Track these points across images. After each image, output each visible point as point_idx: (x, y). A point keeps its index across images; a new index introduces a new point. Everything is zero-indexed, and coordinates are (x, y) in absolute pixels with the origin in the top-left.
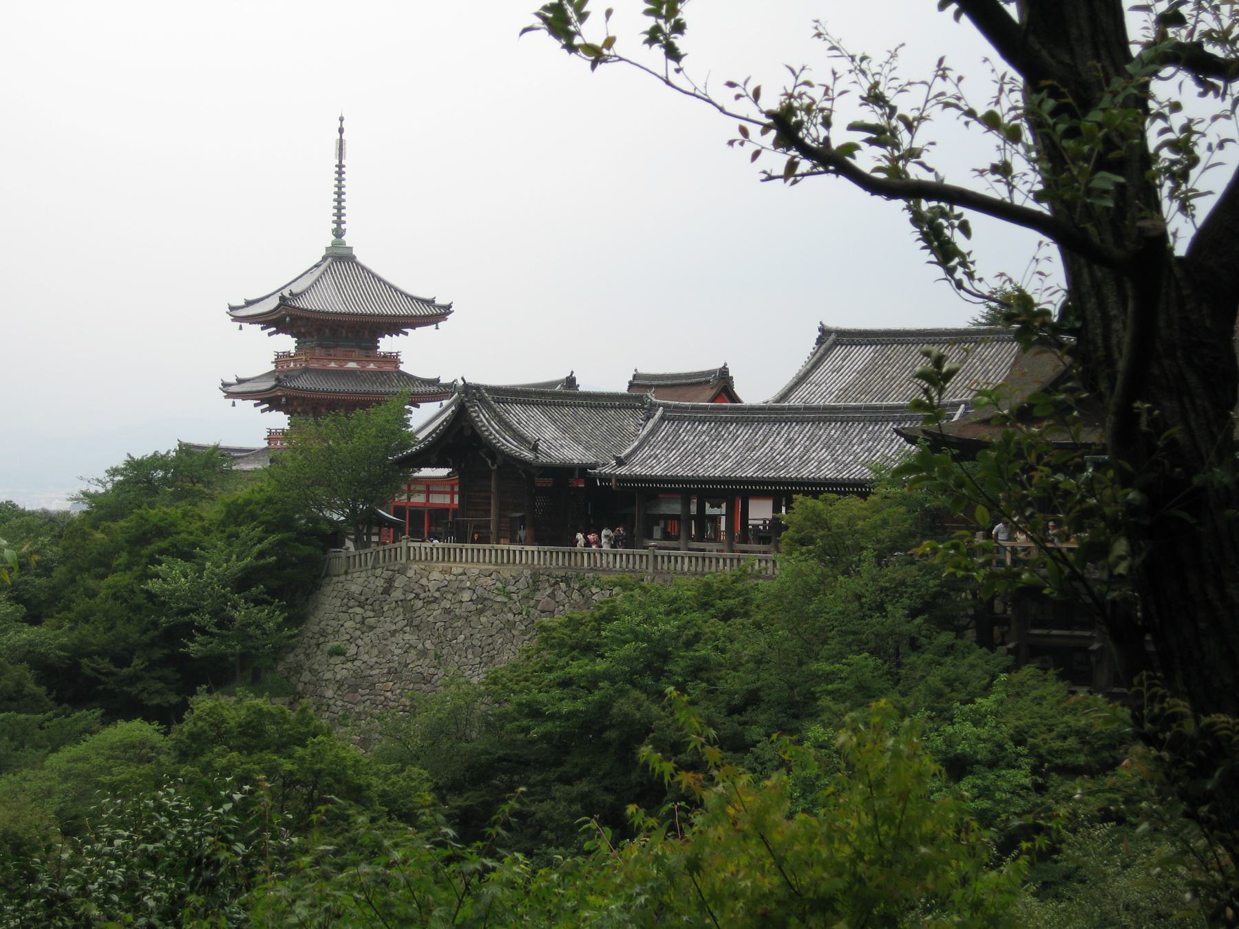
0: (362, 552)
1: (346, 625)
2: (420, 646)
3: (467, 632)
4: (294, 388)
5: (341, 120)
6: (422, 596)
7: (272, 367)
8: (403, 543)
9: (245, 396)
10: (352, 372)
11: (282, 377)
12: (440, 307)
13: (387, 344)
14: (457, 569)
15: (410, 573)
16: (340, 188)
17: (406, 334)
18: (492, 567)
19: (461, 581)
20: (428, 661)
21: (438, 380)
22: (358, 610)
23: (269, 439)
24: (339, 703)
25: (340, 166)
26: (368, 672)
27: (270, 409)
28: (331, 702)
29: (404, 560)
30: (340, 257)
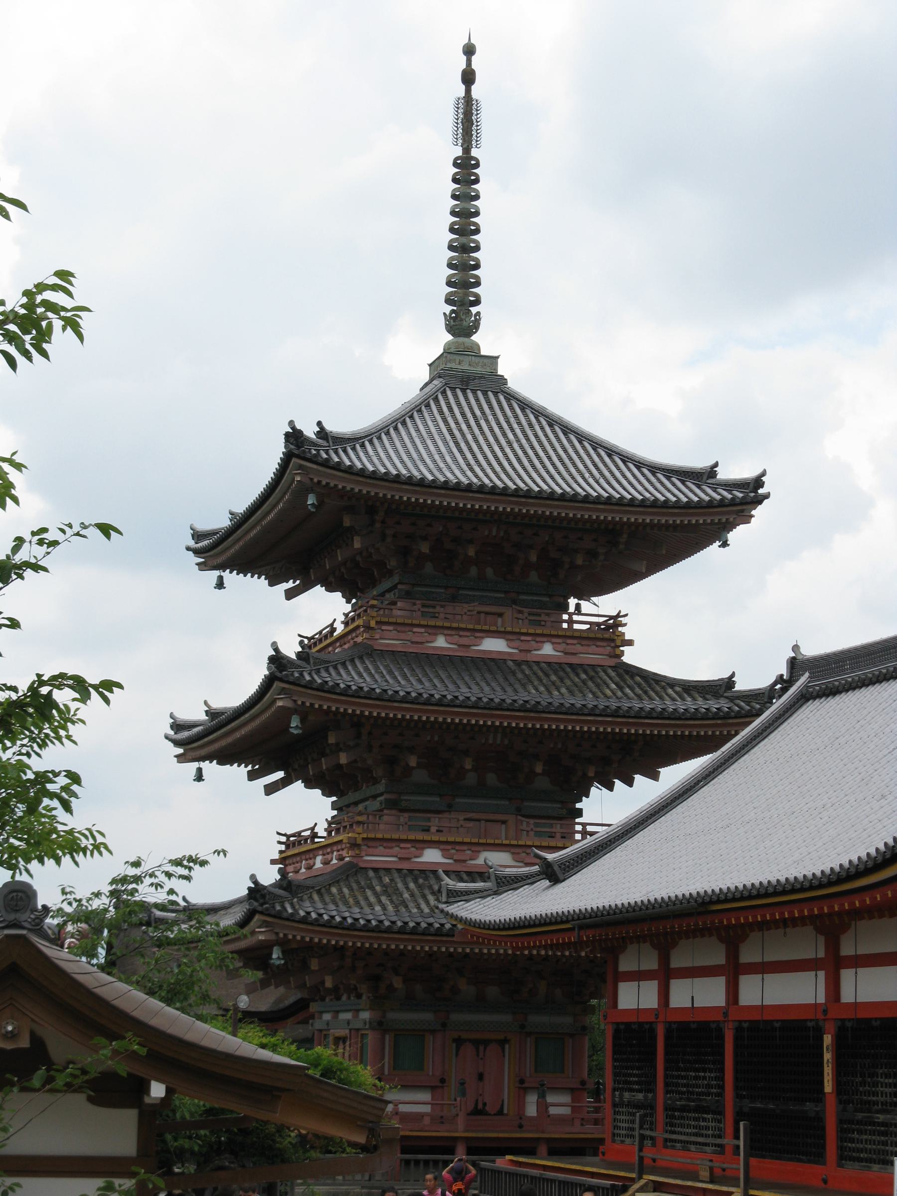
4: (321, 688)
10: (491, 665)
21: (729, 683)
30: (465, 376)
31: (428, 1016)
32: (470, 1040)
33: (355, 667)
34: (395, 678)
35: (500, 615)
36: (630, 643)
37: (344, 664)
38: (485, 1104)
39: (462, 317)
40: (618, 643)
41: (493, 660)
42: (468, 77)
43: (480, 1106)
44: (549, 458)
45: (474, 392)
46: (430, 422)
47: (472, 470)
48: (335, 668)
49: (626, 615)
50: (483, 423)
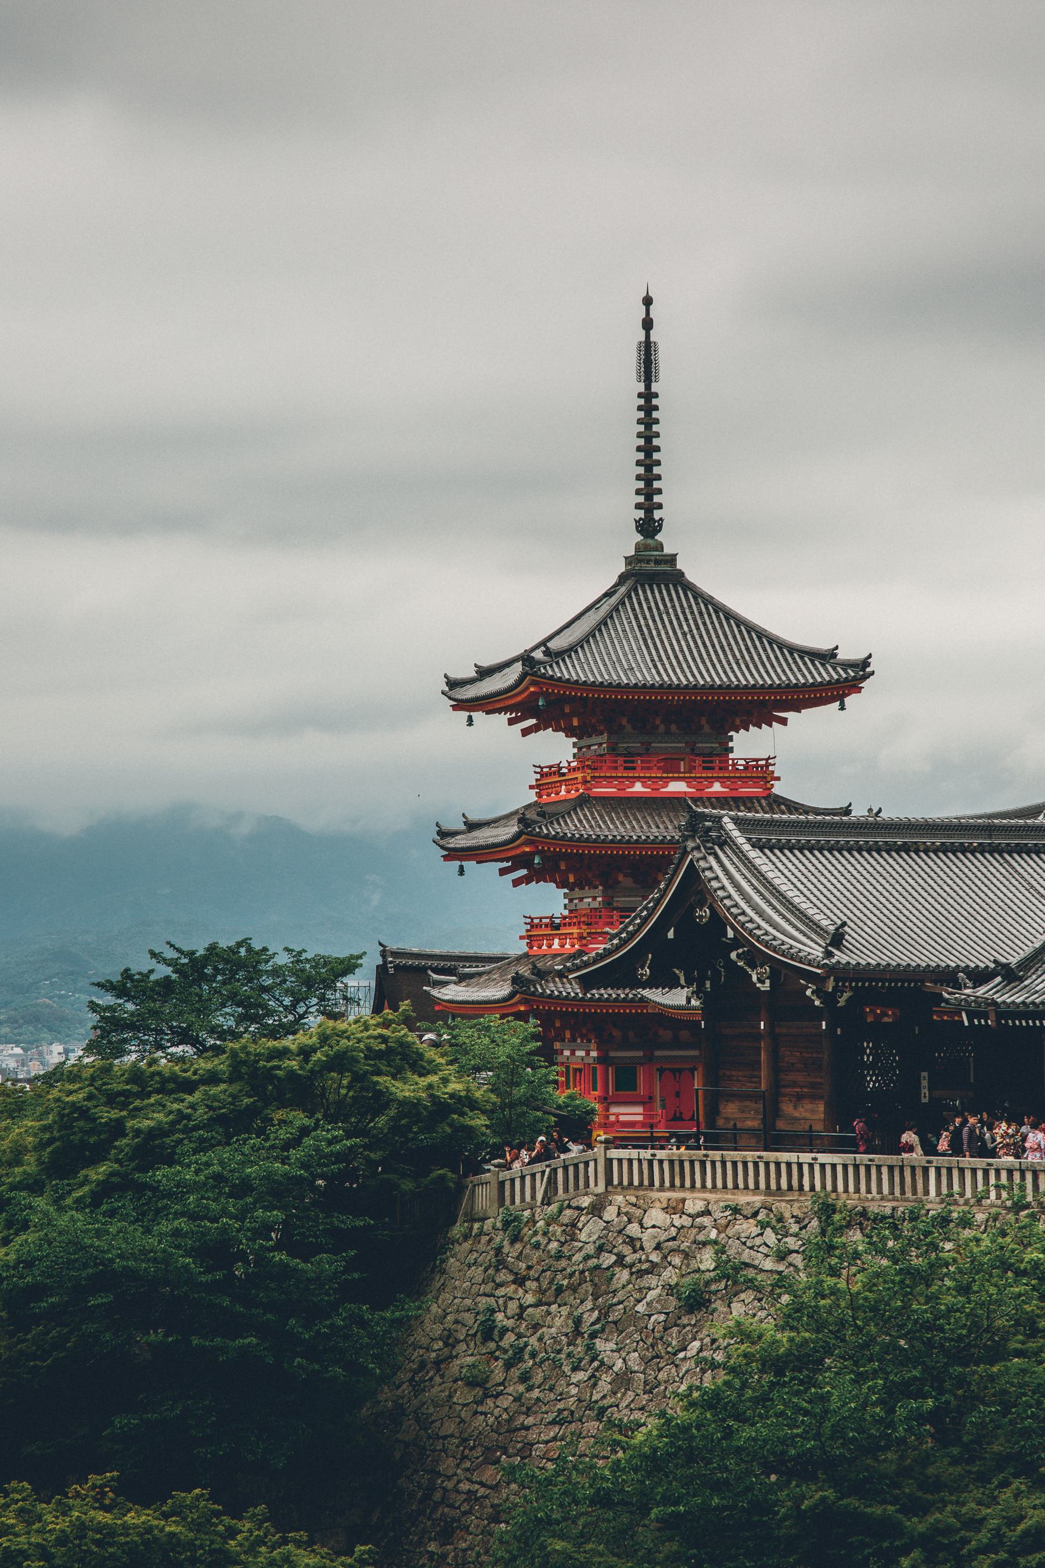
2: (619, 1363)
5: (648, 301)
6: (628, 1260)
7: (532, 797)
8: (598, 1150)
9: (480, 854)
10: (676, 802)
11: (531, 815)
12: (847, 665)
13: (747, 744)
14: (695, 1205)
15: (610, 1213)
16: (648, 439)
17: (784, 722)
18: (758, 1199)
19: (702, 1228)
20: (630, 1394)
23: (531, 939)
24: (465, 1486)
25: (648, 395)
27: (527, 880)
28: (449, 1485)
29: (601, 1188)
30: (652, 572)
31: (640, 1054)
32: (669, 1069)
33: (577, 814)
34: (605, 822)
35: (683, 760)
36: (778, 779)
37: (569, 813)
38: (681, 1113)
40: (769, 779)
42: (648, 324)
43: (678, 1115)
44: (713, 646)
46: (625, 621)
47: (655, 666)
48: (563, 817)
50: (665, 616)
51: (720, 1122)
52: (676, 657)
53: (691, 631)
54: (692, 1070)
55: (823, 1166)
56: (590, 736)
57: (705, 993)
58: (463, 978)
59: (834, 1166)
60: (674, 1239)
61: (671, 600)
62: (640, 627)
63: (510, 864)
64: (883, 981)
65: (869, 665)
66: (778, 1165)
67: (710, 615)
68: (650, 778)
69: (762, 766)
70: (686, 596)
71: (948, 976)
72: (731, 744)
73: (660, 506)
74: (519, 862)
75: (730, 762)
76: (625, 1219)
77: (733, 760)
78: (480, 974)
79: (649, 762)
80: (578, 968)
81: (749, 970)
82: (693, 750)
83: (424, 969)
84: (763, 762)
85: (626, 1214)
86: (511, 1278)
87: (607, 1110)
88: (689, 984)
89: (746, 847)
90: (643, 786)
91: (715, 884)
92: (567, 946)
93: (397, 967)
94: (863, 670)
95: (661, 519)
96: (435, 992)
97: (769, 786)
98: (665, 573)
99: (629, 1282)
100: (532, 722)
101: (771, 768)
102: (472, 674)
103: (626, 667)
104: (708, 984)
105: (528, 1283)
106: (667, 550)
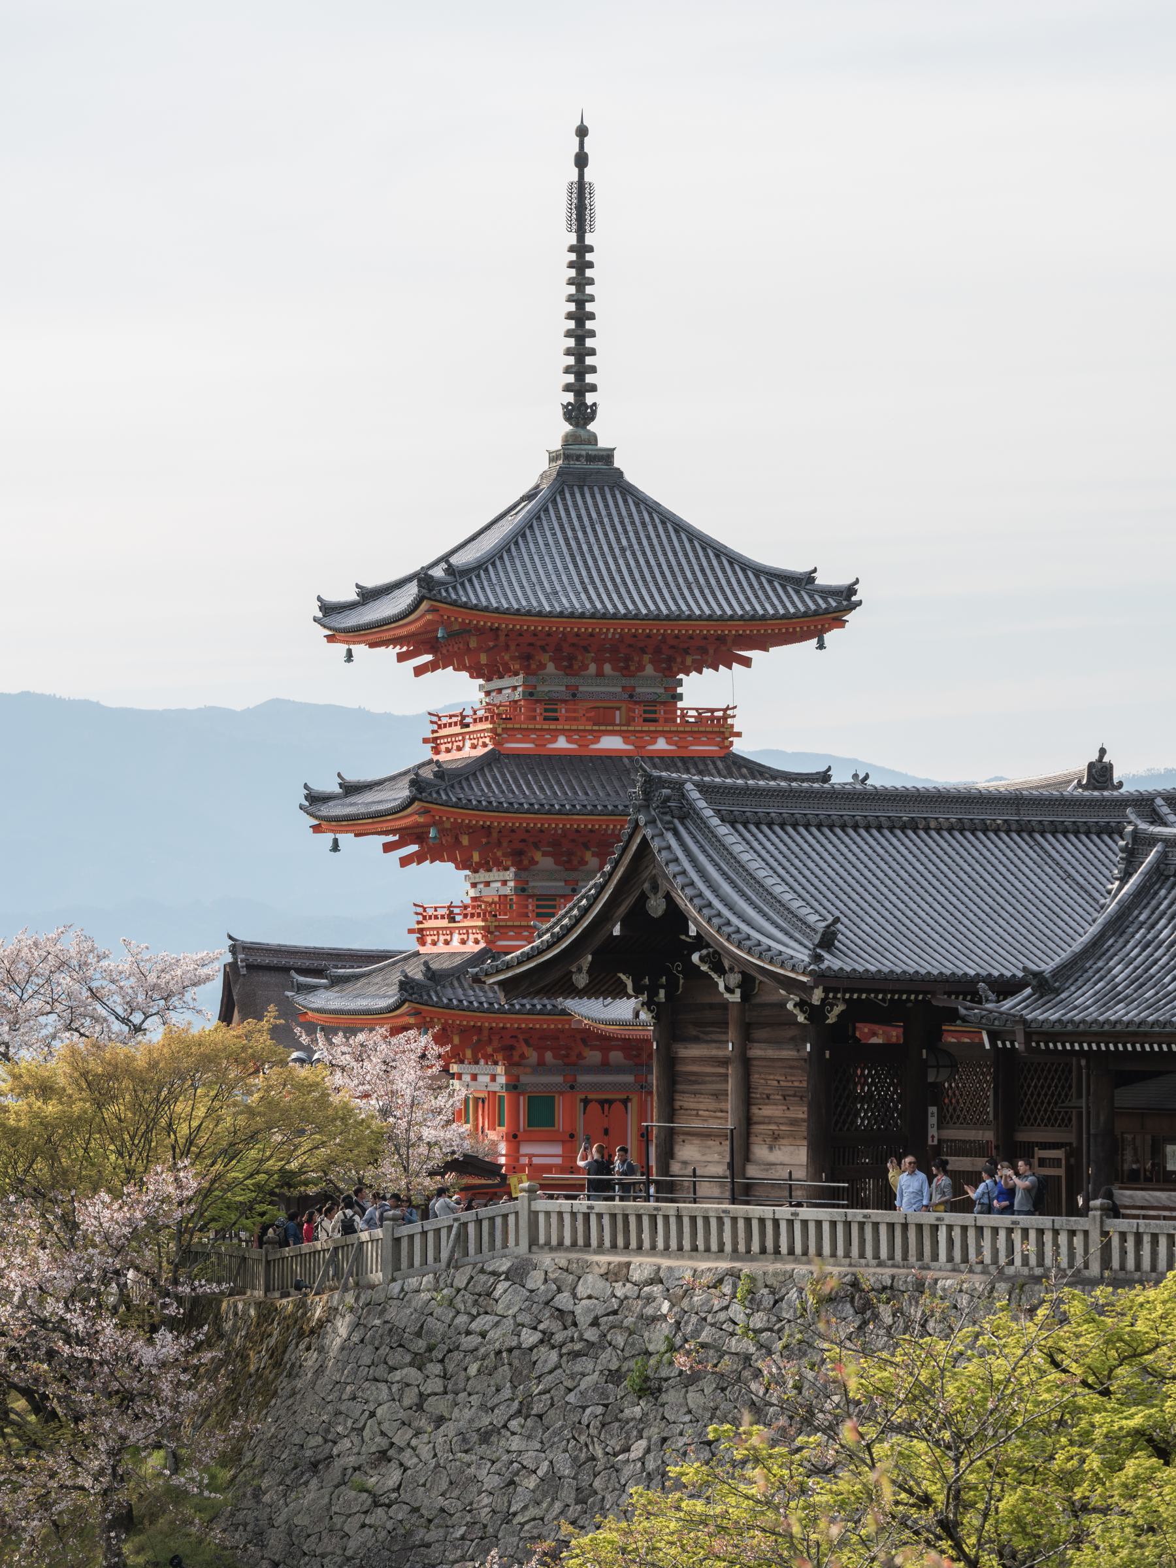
0: (484, 1212)
1: (379, 1412)
3: (654, 1432)
5: (582, 132)
6: (559, 1338)
9: (360, 824)
10: (610, 760)
13: (700, 690)
15: (535, 1280)
17: (747, 662)
18: (724, 1265)
19: (650, 1299)
22: (412, 1373)
25: (581, 249)
26: (420, 1535)
27: (419, 858)
30: (585, 472)
31: (559, 1079)
33: (484, 776)
34: (519, 787)
35: (618, 709)
36: (739, 735)
39: (580, 413)
40: (727, 735)
41: (610, 757)
42: (581, 160)
44: (659, 565)
45: (591, 489)
46: (548, 534)
48: (467, 779)
49: (735, 707)
51: (675, 1168)
52: (613, 579)
53: (631, 546)
54: (625, 1102)
55: (805, 1223)
56: (501, 677)
57: (658, 1004)
58: (338, 982)
59: (819, 1223)
60: (615, 1313)
61: (607, 506)
62: (566, 540)
63: (397, 838)
64: (885, 992)
65: (855, 592)
66: (748, 1221)
67: (655, 527)
68: (577, 731)
69: (719, 719)
70: (625, 501)
71: (966, 987)
72: (679, 690)
73: (593, 388)
74: (408, 835)
75: (679, 712)
76: (554, 1287)
77: (682, 709)
78: (357, 977)
79: (575, 711)
80: (498, 971)
81: (714, 976)
82: (631, 696)
83: (286, 970)
84: (720, 714)
85: (555, 1281)
86: (408, 1358)
87: (518, 1150)
88: (638, 991)
89: (715, 821)
90: (568, 741)
91: (672, 869)
92: (470, 943)
93: (249, 967)
94: (848, 598)
95: (595, 404)
96: (301, 1000)
97: (726, 743)
98: (599, 472)
99: (558, 1366)
100: (428, 658)
101: (730, 721)
102: (352, 596)
103: (549, 590)
104: (662, 993)
105: (429, 1366)
106: (603, 443)
